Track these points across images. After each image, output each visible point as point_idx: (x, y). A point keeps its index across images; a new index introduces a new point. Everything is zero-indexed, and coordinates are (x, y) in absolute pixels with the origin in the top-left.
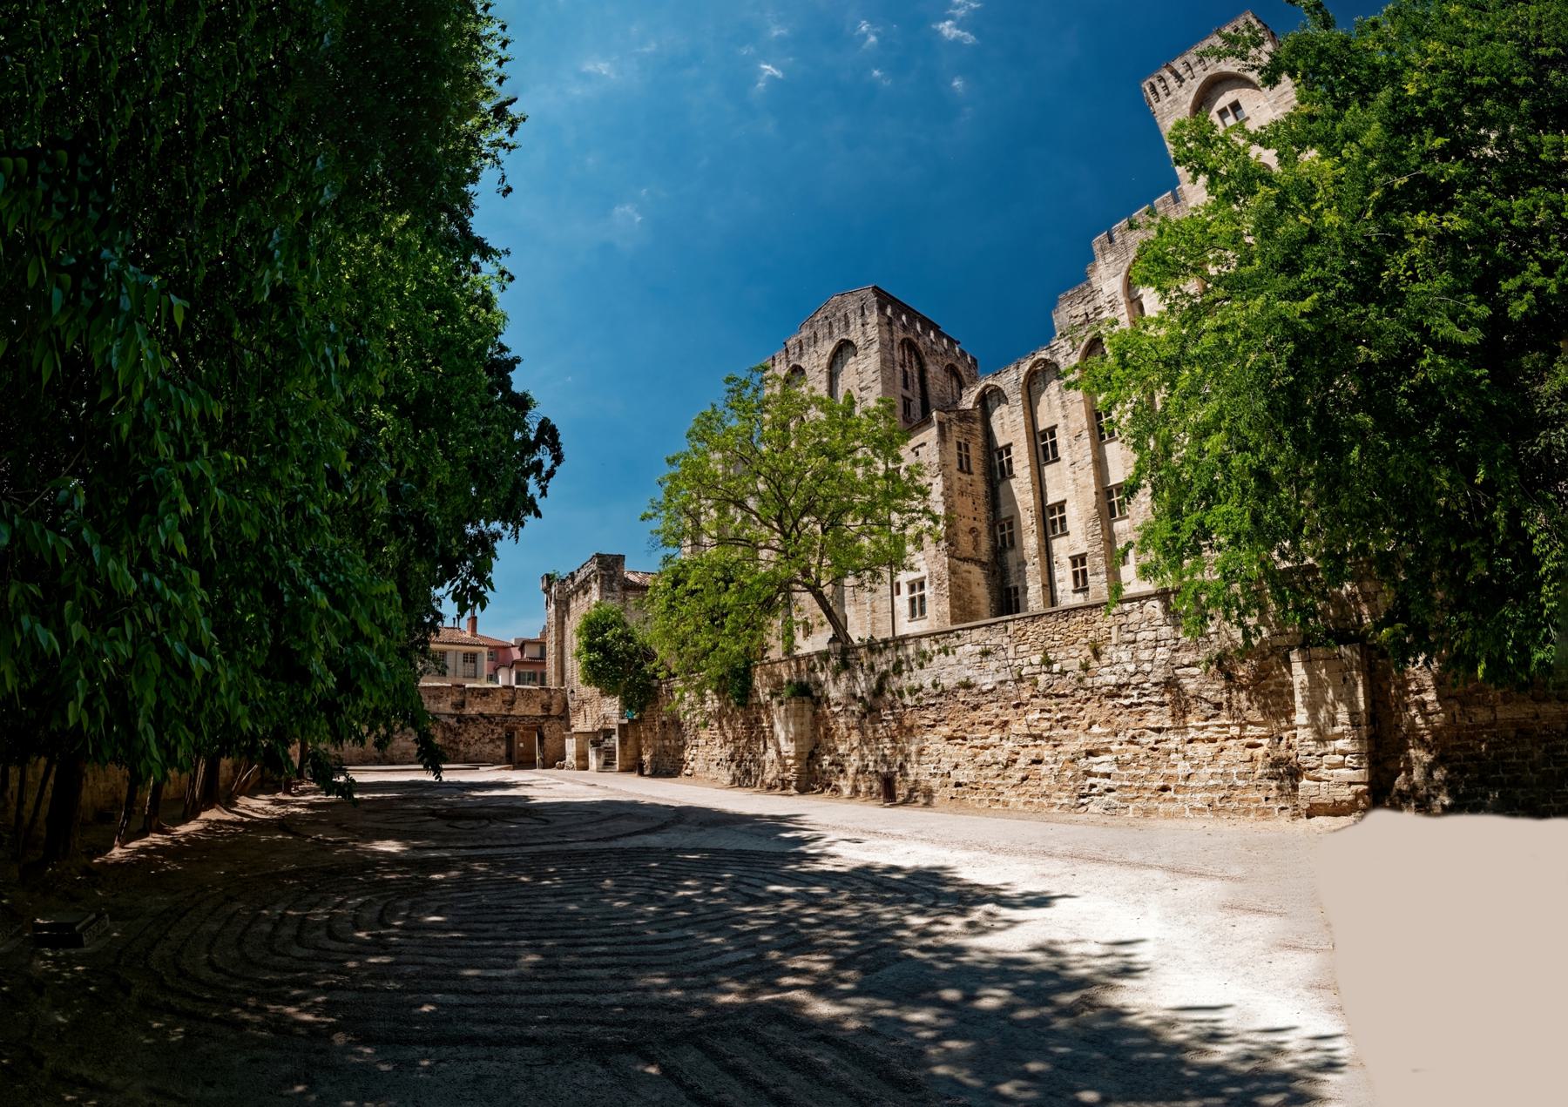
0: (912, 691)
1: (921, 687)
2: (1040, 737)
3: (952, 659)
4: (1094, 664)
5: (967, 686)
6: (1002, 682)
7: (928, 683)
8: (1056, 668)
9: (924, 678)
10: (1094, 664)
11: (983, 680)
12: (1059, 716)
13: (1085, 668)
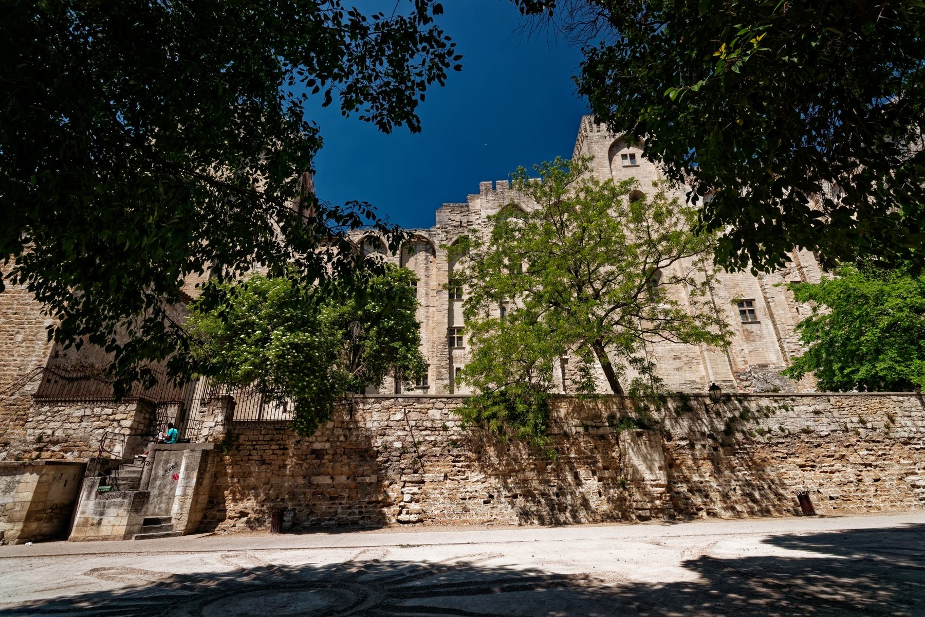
0: (762, 433)
1: (769, 431)
2: (870, 465)
3: (791, 413)
4: (892, 425)
5: (807, 431)
6: (832, 431)
7: (775, 428)
8: (869, 425)
9: (772, 424)
10: (892, 425)
11: (819, 429)
12: (880, 453)
13: (887, 427)
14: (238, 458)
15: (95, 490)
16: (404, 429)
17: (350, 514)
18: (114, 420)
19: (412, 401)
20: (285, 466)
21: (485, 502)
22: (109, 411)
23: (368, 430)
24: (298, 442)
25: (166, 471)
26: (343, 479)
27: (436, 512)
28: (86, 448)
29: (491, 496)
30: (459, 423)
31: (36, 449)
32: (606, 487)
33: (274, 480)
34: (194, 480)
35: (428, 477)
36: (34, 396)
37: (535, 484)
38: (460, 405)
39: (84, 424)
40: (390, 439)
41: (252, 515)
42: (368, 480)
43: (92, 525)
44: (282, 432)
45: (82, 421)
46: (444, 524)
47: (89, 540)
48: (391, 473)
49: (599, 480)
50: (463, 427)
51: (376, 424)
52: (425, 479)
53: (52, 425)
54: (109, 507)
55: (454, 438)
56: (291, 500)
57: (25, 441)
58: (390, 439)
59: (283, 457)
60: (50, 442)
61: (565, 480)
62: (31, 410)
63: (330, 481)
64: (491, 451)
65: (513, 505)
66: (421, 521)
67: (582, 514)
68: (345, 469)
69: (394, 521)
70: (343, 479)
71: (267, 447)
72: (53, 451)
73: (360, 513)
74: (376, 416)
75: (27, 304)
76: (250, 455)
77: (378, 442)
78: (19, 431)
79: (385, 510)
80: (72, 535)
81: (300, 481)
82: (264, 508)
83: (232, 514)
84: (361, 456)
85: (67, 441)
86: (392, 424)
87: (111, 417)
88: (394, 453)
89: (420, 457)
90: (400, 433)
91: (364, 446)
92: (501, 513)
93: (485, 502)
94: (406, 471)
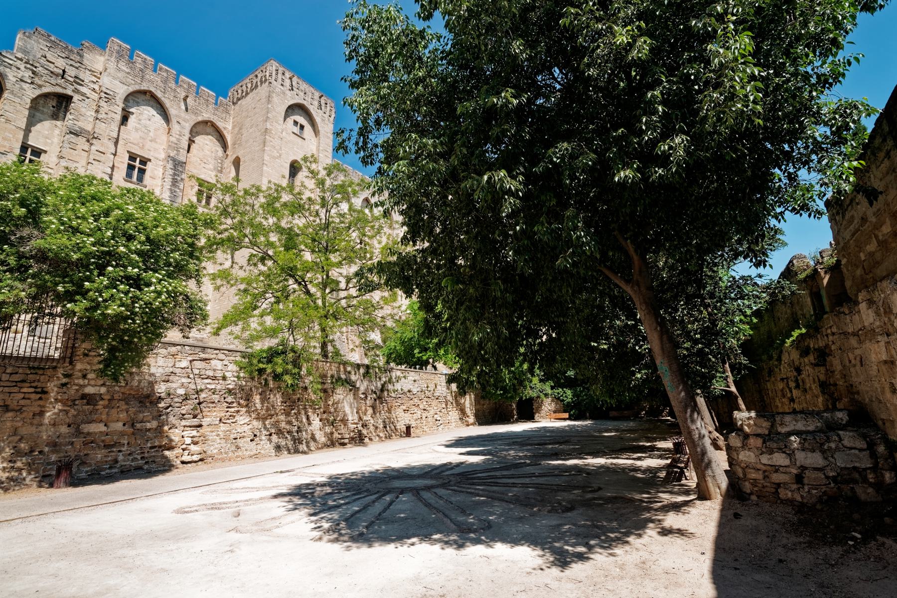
9: (398, 386)
16: (189, 377)
17: (132, 460)
19: (198, 350)
20: (42, 413)
21: (252, 440)
23: (151, 375)
24: (64, 385)
26: (119, 426)
27: (215, 451)
29: (255, 436)
30: (236, 374)
32: (324, 425)
33: (25, 431)
35: (205, 422)
37: (283, 425)
38: (238, 359)
40: (174, 385)
42: (148, 425)
44: (41, 372)
46: (223, 460)
48: (172, 419)
49: (321, 420)
50: (238, 377)
51: (160, 370)
52: (203, 424)
55: (231, 387)
56: (53, 452)
58: (174, 385)
59: (41, 403)
61: (301, 422)
63: (104, 429)
64: (257, 399)
65: (270, 440)
66: (201, 460)
67: (312, 444)
68: (123, 415)
69: (179, 462)
70: (119, 426)
71: (16, 389)
73: (142, 458)
74: (161, 361)
77: (161, 389)
79: (167, 453)
81: (64, 429)
82: (19, 464)
84: (140, 402)
86: (177, 371)
88: (176, 400)
89: (199, 404)
90: (185, 380)
91: (146, 391)
92: (263, 448)
93: (252, 440)
94: (186, 416)
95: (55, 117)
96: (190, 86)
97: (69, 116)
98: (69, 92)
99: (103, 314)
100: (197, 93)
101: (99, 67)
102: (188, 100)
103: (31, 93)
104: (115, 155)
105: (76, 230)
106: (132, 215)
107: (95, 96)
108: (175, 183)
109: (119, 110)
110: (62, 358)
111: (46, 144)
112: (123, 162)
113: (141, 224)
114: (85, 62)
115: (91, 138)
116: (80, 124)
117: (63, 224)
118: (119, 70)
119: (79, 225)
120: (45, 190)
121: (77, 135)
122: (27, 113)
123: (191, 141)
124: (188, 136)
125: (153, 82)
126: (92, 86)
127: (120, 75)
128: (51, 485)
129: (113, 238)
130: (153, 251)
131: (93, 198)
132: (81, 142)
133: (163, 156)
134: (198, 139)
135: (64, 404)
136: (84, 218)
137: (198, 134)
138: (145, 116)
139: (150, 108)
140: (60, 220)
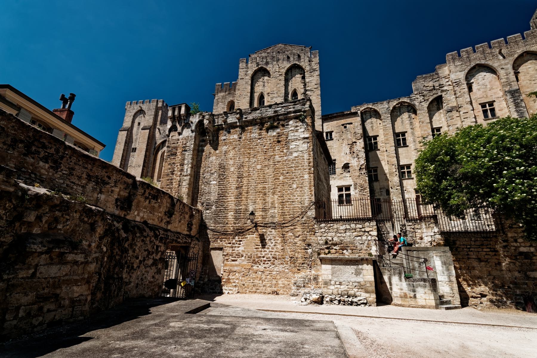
14: (460, 257)
15: (403, 275)
18: (365, 231)
20: (500, 264)
22: (361, 226)
24: (505, 247)
25: (420, 264)
28: (355, 248)
31: (327, 248)
33: (495, 273)
34: (454, 272)
36: (315, 218)
39: (348, 234)
41: (490, 297)
43: (411, 298)
44: (489, 240)
45: (345, 232)
47: (412, 307)
53: (330, 234)
54: (417, 287)
57: (319, 244)
60: (332, 244)
62: (316, 226)
71: (480, 250)
72: (336, 250)
75: (292, 167)
76: (468, 255)
78: (313, 238)
80: (395, 301)
81: (517, 274)
83: (474, 295)
85: (341, 244)
87: (363, 230)
95: (439, 109)
96: (499, 43)
97: (444, 105)
98: (440, 94)
99: (512, 200)
100: (507, 43)
101: (447, 72)
102: (503, 51)
103: (425, 105)
104: (473, 110)
105: (476, 158)
106: (504, 135)
107: (451, 87)
108: (517, 105)
109: (465, 86)
110: (498, 230)
111: (440, 124)
112: (479, 110)
113: (512, 139)
114: (440, 75)
115: (457, 108)
116: (450, 105)
117: (468, 157)
118: (456, 66)
119: (477, 154)
120: (452, 143)
121: (451, 111)
122: (428, 115)
123: (517, 74)
124: (512, 72)
125: (477, 58)
126: (448, 84)
127: (458, 69)
128: (524, 310)
129: (498, 153)
130: (528, 152)
131: (477, 136)
132: (455, 114)
133: (501, 94)
134: (522, 69)
135: (511, 259)
136: (478, 149)
137: (519, 66)
138: (482, 79)
139: (481, 73)
140: (466, 155)
